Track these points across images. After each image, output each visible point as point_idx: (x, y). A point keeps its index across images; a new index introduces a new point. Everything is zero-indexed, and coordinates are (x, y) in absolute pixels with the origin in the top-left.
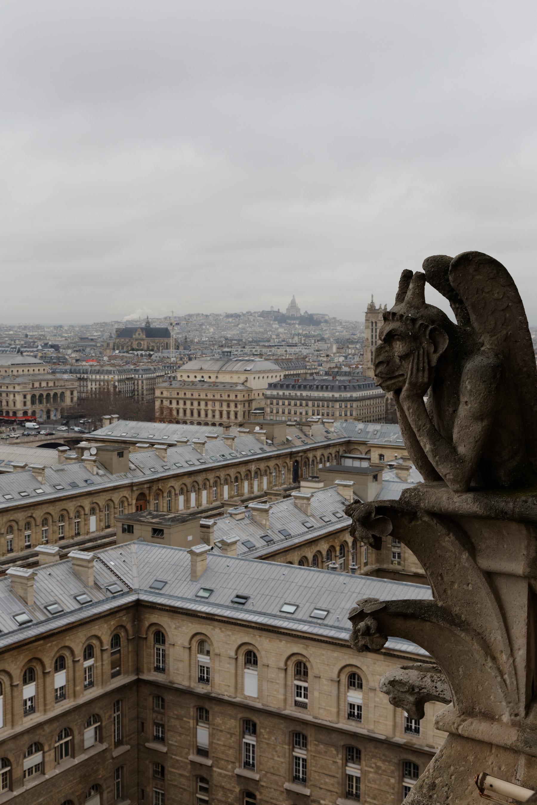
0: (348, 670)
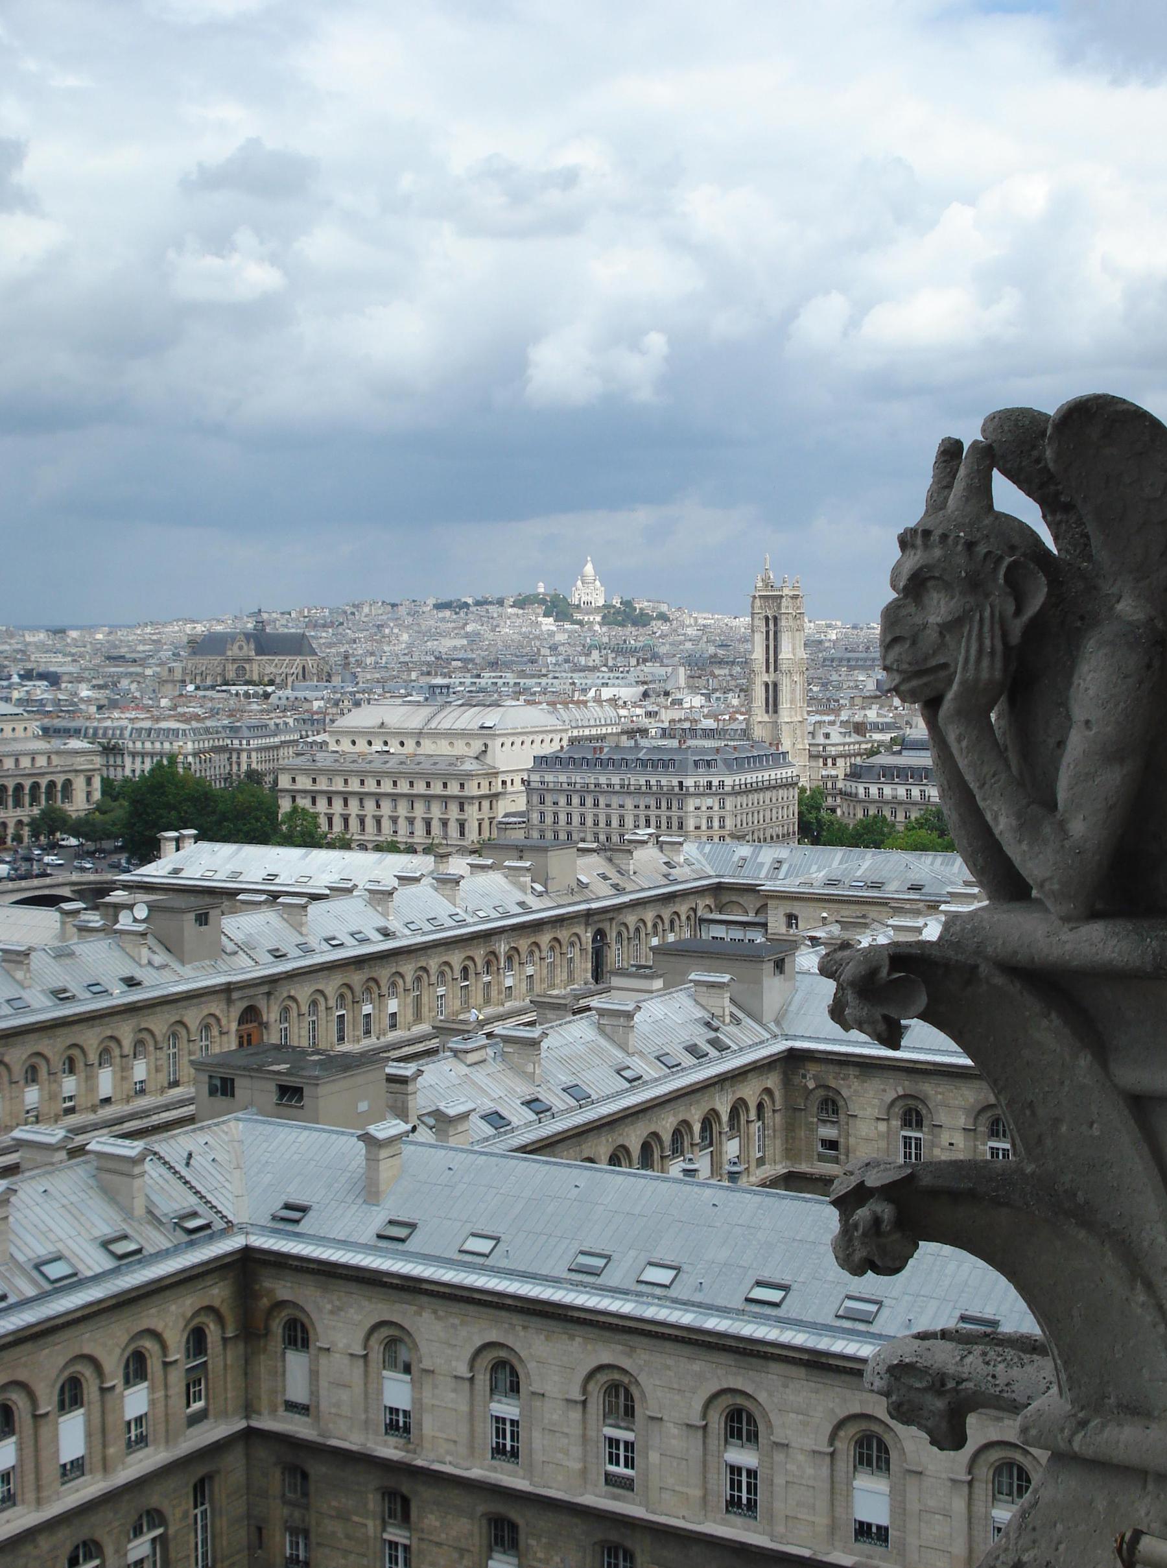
0: (726, 1401)
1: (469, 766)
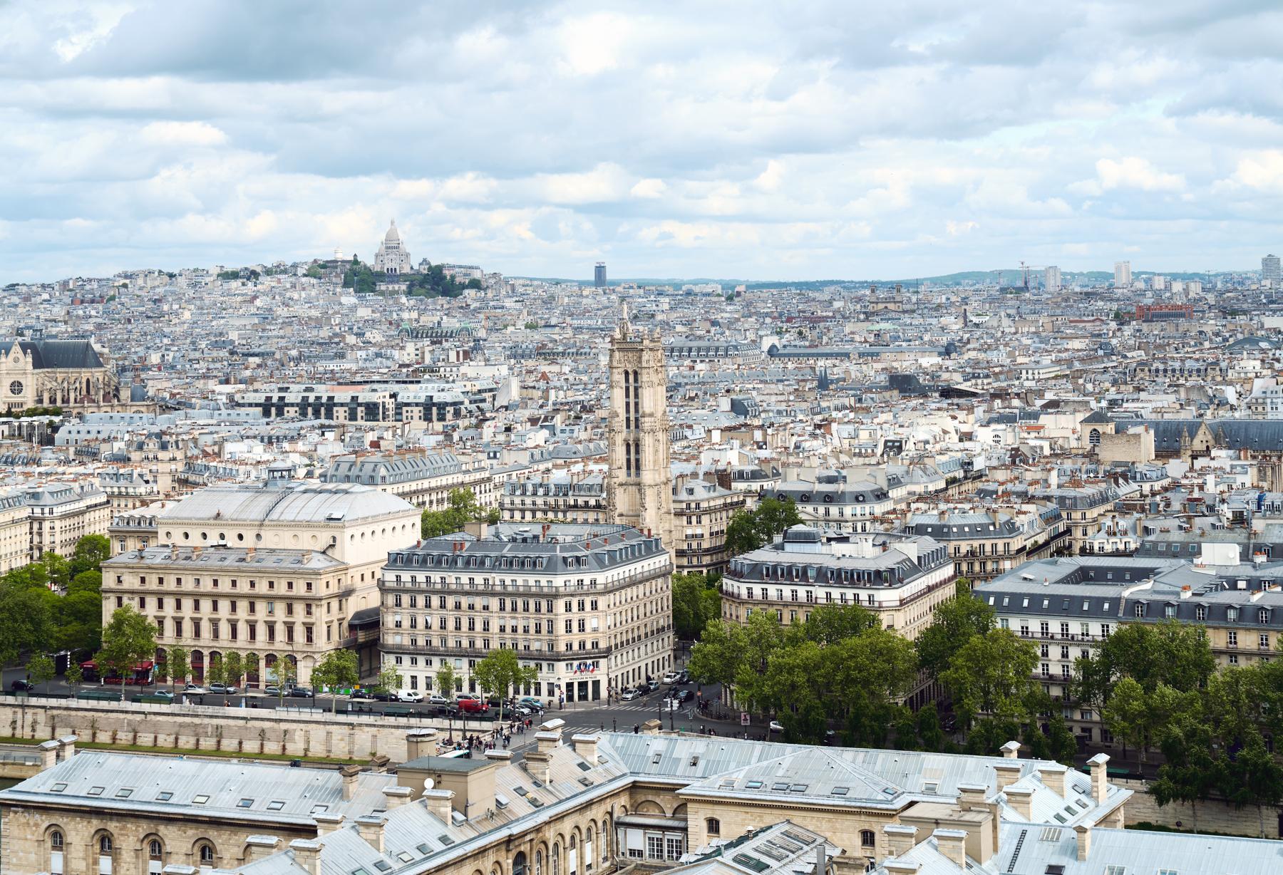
1: (317, 562)
